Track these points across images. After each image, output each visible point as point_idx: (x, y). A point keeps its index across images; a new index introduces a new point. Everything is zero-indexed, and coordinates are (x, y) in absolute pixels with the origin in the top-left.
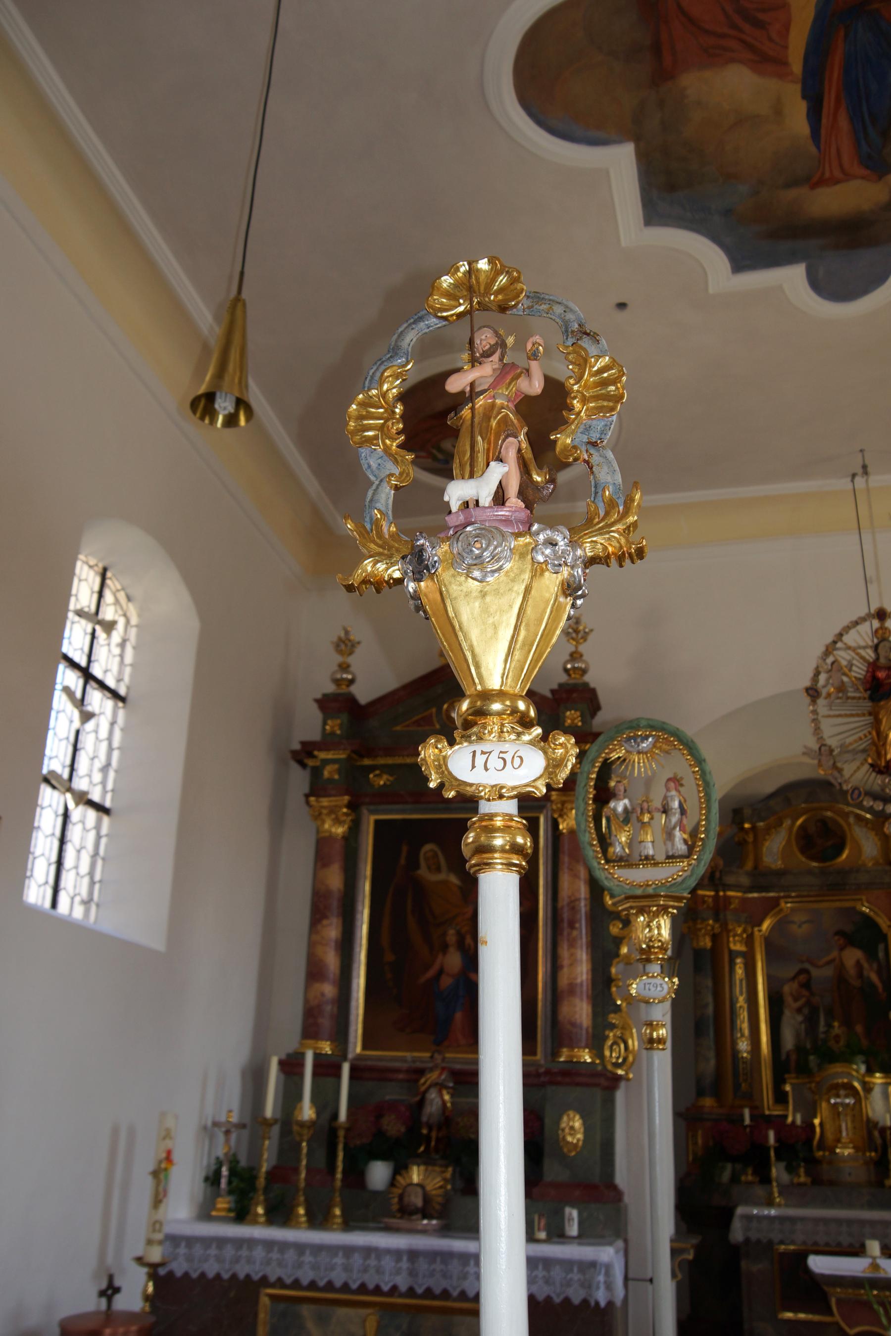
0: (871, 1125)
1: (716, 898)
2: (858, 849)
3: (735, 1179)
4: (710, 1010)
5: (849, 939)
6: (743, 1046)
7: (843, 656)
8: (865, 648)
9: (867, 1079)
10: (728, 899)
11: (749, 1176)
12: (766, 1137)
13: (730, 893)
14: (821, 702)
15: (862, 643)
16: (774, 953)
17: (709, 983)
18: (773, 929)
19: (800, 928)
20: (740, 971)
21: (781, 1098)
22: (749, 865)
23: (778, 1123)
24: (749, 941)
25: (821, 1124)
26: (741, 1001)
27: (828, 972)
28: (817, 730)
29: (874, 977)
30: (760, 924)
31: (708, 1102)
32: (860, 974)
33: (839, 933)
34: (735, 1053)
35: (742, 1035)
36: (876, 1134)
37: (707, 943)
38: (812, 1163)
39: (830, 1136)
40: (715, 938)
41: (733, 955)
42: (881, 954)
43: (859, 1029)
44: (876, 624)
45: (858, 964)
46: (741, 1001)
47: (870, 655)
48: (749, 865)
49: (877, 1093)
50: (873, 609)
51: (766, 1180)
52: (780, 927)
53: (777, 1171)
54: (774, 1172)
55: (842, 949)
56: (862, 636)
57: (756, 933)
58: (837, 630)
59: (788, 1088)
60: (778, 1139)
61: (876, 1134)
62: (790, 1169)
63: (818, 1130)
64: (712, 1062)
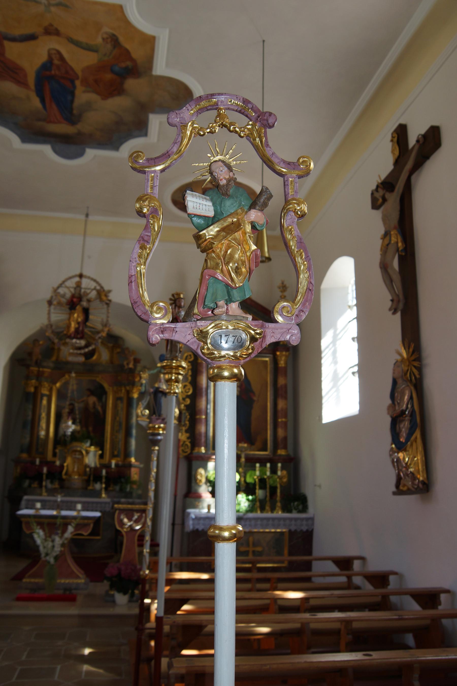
0: (87, 466)
1: (39, 371)
2: (100, 355)
3: (30, 486)
4: (30, 418)
5: (92, 392)
6: (43, 433)
7: (61, 291)
8: (72, 288)
9: (88, 449)
10: (43, 372)
11: (35, 485)
12: (42, 470)
13: (45, 370)
14: (52, 307)
15: (72, 286)
16: (61, 396)
17: (31, 406)
18: (61, 386)
19: (73, 386)
20: (45, 402)
21: (54, 455)
22: (54, 358)
23: (50, 464)
24: (51, 390)
25: (67, 466)
26: (44, 415)
27: (82, 405)
28: (49, 318)
29: (99, 408)
30: (55, 383)
31: (24, 455)
32: (94, 407)
33: (89, 390)
34: (38, 436)
35: (42, 429)
36: (88, 469)
37: (32, 390)
38: (61, 480)
39: (70, 469)
40: (36, 388)
41: (43, 395)
42: (104, 399)
43: (91, 429)
44: (77, 279)
45: (94, 404)
46: (44, 415)
47: (72, 290)
48: (54, 358)
49: (91, 455)
50: (78, 272)
51: (41, 486)
52: (66, 385)
53: (47, 483)
54: (44, 483)
55: (88, 396)
56: (72, 283)
57: (54, 388)
58: (63, 279)
59: (57, 451)
60: (48, 471)
61: (88, 469)
62: (52, 482)
63: (65, 469)
64: (27, 440)
